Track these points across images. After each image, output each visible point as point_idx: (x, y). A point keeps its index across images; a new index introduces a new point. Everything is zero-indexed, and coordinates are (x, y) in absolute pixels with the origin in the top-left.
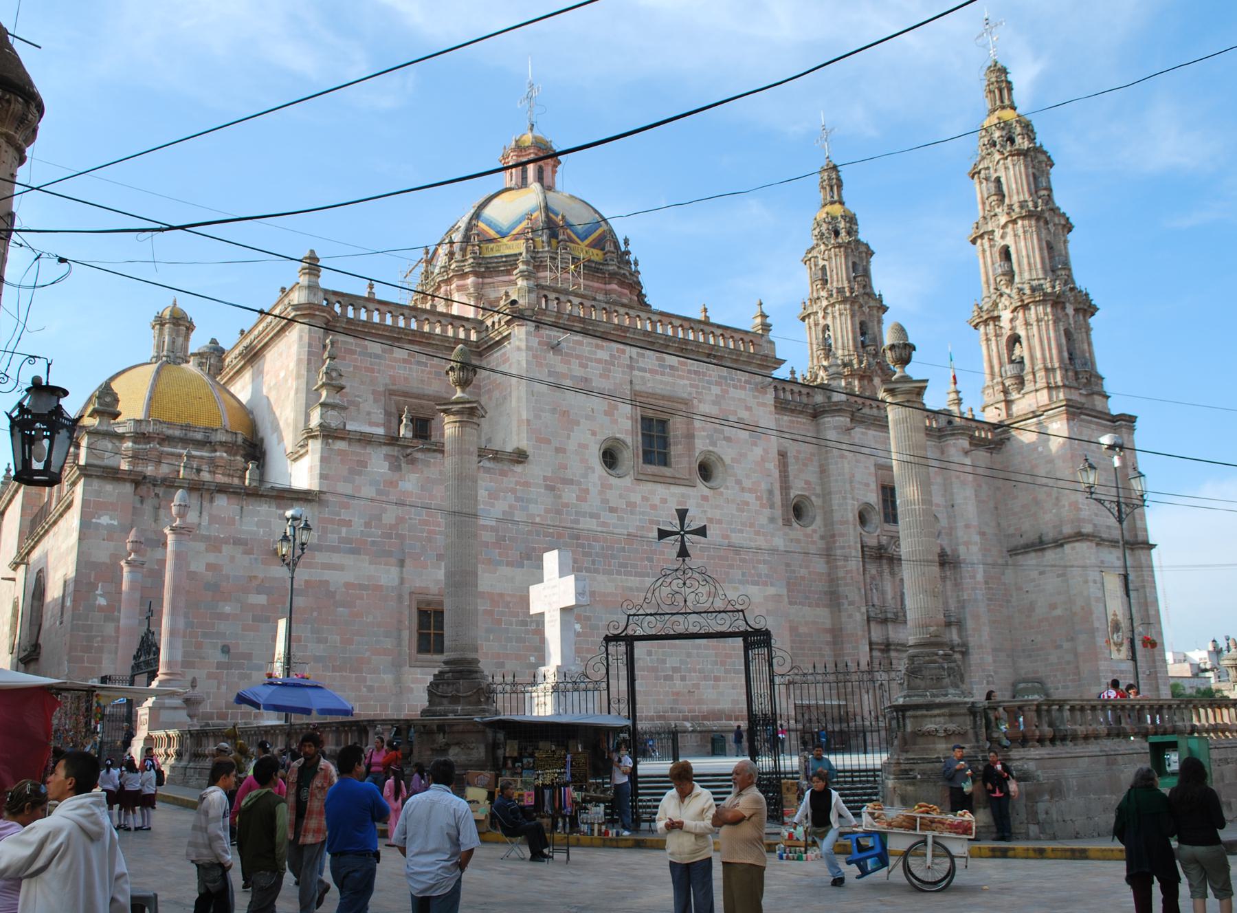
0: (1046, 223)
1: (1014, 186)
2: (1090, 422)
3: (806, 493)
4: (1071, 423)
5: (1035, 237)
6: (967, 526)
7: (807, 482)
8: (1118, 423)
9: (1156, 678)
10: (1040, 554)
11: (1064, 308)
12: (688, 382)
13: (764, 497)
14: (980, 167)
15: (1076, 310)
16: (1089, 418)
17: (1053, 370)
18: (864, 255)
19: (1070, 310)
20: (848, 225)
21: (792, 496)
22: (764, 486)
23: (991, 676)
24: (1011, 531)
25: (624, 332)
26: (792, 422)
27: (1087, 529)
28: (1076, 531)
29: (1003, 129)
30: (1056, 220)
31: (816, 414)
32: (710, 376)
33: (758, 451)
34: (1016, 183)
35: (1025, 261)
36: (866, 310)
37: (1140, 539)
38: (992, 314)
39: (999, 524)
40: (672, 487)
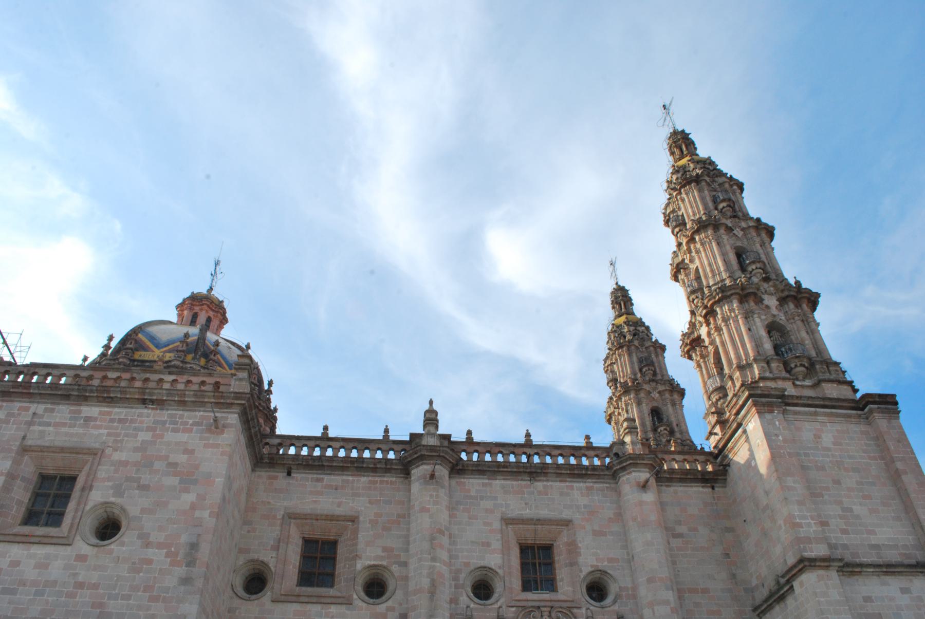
0: (729, 230)
1: (690, 210)
2: (816, 414)
3: (384, 563)
4: (768, 416)
5: (714, 244)
6: (650, 580)
7: (385, 549)
8: (866, 410)
10: (782, 605)
11: (759, 301)
12: (106, 431)
13: (182, 552)
14: (667, 213)
15: (782, 301)
17: (749, 365)
18: (652, 348)
19: (771, 301)
20: (632, 328)
21: (359, 566)
22: (184, 539)
24: (754, 582)
25: (25, 388)
26: (375, 482)
27: (819, 550)
28: (798, 557)
29: (678, 172)
30: (743, 224)
31: (404, 468)
32: (142, 422)
33: (189, 498)
34: (692, 207)
35: (708, 269)
36: (656, 395)
38: (692, 337)
39: (734, 576)
40: (35, 546)
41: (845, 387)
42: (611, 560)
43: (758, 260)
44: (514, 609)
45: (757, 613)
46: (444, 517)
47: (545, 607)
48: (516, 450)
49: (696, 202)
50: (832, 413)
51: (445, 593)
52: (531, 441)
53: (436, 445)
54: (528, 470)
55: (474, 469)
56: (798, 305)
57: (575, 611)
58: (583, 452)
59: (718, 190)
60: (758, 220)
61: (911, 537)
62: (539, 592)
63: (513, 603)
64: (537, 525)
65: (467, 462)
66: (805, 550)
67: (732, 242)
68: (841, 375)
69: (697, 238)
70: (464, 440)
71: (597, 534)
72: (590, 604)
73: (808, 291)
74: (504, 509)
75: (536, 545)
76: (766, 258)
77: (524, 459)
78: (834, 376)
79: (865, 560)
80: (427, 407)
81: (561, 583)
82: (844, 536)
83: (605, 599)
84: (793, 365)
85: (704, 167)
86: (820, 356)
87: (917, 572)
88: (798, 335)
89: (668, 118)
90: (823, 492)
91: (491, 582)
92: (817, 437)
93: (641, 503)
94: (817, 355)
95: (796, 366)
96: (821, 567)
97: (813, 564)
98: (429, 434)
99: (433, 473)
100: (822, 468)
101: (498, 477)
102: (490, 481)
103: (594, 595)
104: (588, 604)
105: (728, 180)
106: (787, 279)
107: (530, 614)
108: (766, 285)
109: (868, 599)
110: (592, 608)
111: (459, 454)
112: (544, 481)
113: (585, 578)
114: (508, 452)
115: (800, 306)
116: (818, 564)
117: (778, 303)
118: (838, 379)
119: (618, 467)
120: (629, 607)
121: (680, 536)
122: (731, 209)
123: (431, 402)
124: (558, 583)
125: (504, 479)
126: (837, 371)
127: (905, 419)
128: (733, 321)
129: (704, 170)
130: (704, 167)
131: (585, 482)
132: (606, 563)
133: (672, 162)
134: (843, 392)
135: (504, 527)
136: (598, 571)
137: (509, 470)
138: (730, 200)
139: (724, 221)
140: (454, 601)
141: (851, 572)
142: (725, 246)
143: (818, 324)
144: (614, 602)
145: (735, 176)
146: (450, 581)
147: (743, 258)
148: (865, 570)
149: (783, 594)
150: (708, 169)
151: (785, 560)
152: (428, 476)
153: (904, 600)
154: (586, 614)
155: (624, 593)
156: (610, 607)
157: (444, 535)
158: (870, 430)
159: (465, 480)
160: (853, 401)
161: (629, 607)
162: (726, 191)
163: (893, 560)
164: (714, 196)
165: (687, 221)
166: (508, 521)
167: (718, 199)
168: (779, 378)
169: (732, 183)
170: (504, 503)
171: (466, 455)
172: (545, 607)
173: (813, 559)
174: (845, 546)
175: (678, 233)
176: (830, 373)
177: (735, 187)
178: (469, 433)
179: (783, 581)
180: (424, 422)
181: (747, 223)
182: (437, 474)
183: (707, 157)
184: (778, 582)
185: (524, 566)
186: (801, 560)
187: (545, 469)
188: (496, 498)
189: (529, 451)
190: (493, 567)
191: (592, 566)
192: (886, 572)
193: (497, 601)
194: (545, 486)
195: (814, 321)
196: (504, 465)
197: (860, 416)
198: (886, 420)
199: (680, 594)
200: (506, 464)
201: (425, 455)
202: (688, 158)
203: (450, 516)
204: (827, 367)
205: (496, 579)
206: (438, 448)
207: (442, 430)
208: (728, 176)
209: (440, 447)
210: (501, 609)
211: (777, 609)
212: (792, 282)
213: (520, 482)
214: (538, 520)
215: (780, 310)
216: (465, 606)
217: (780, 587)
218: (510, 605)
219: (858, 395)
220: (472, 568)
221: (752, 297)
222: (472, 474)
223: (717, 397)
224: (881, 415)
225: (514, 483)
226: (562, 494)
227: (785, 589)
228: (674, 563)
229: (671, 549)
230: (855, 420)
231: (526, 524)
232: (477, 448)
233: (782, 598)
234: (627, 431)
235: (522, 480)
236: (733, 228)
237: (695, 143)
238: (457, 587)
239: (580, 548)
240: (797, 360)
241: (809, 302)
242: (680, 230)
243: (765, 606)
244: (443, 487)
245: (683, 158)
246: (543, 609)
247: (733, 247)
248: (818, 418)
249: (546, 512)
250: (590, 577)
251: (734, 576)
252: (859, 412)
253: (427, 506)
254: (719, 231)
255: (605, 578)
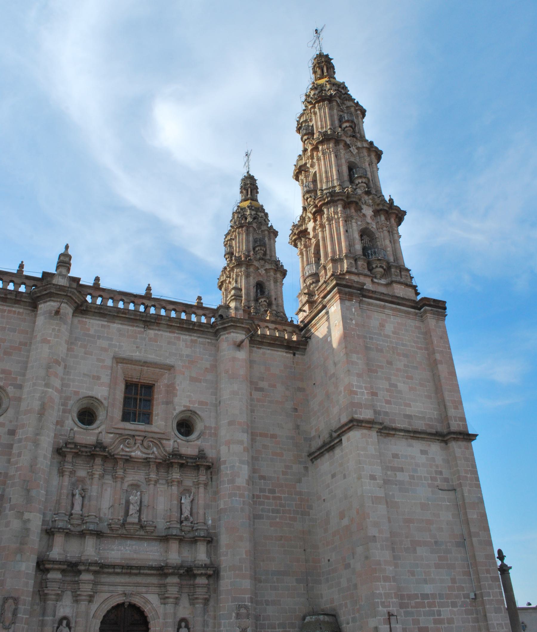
0: (347, 146)
1: (319, 123)
2: (384, 307)
4: (347, 303)
6: (230, 423)
8: (422, 310)
9: (483, 603)
11: (359, 209)
14: (301, 121)
15: (377, 213)
16: (383, 303)
17: (341, 260)
19: (368, 211)
23: (246, 607)
27: (366, 414)
28: (350, 418)
29: (316, 89)
30: (359, 144)
34: (321, 121)
35: (324, 175)
36: (262, 271)
37: (455, 426)
38: (300, 229)
41: (410, 290)
42: (201, 403)
43: (365, 176)
44: (112, 435)
45: (311, 458)
46: (62, 349)
47: (139, 436)
48: (136, 301)
49: (325, 117)
50: (396, 308)
51: (53, 415)
52: (151, 294)
53: (65, 285)
54: (144, 319)
55: (96, 311)
56: (388, 219)
57: (164, 442)
58: (193, 310)
59: (345, 111)
60: (371, 143)
61: (435, 413)
62: (136, 423)
63: (112, 430)
64: (144, 366)
65: (91, 305)
66: (356, 413)
67: (348, 157)
68: (409, 280)
69: (320, 148)
70: (92, 285)
71: (193, 380)
72: (178, 437)
73: (397, 208)
74: (117, 350)
75: (140, 384)
76: (371, 176)
77: (142, 309)
78: (404, 279)
79: (399, 425)
80: (63, 250)
81: (156, 418)
82: (387, 405)
83: (192, 434)
84: (374, 266)
85: (338, 90)
86: (396, 262)
87: (435, 439)
88: (383, 243)
89: (317, 42)
90: (378, 369)
91: (95, 410)
92: (382, 326)
93: (234, 359)
94: (394, 260)
95: (377, 267)
96: (366, 428)
97: (360, 424)
98: (60, 274)
99: (59, 310)
100: (381, 351)
101: (116, 321)
102: (109, 324)
103: (182, 430)
104: (176, 437)
105: (354, 105)
106: (383, 196)
107: (125, 441)
108: (366, 197)
109: (395, 456)
110: (179, 441)
111: (84, 296)
112: (156, 330)
113: (178, 415)
114: (128, 301)
115: (389, 219)
116: (363, 425)
117: (373, 214)
118: (406, 282)
119: (221, 327)
120: (210, 443)
121: (261, 390)
122: (352, 130)
123: (67, 247)
124: (153, 418)
125: (121, 324)
126: (406, 276)
127: (449, 321)
128: (336, 222)
129: (337, 92)
130: (338, 90)
131: (191, 336)
132: (196, 405)
133: (313, 80)
134: (408, 293)
135: (115, 365)
136: (189, 410)
137: (127, 316)
138: (352, 122)
139: (344, 138)
140: (60, 423)
141: (387, 434)
142: (341, 159)
143: (400, 237)
144: (198, 438)
145: (361, 103)
146: (59, 405)
147: (353, 172)
148: (398, 433)
149: (333, 445)
150: (341, 92)
151: (340, 419)
152: (54, 312)
153: (422, 459)
154: (174, 445)
155: (207, 432)
156: (194, 441)
157: (60, 366)
158: (422, 326)
159: (87, 320)
160: (414, 301)
161: (210, 443)
162: (351, 114)
163: (420, 428)
164: (341, 116)
165: (315, 131)
166: (119, 360)
167: (343, 119)
168: (362, 274)
169: (357, 108)
170: (118, 344)
171: (91, 298)
172: (139, 436)
173: (361, 420)
174: (386, 413)
175: (306, 140)
176: (401, 277)
177: (359, 112)
178: (97, 279)
179: (335, 435)
180: (58, 263)
181: (362, 144)
182: (61, 311)
183: (342, 82)
184: (331, 436)
185: (127, 400)
186: (352, 421)
187: (158, 320)
188: (111, 339)
189: (147, 302)
190: (99, 398)
191: (185, 406)
192: (413, 437)
193: (98, 427)
194: (155, 334)
195: (398, 233)
196: (123, 312)
197: (416, 314)
198: (435, 320)
199: (253, 436)
200: (126, 311)
201: (53, 293)
202: (326, 79)
203: (68, 350)
204: (400, 271)
205: (100, 409)
206: (67, 289)
207: (73, 273)
208: (356, 101)
209: (69, 288)
210: (101, 434)
211: (327, 456)
212: (387, 199)
213: (135, 328)
214: (145, 362)
215: (373, 220)
216: (69, 429)
217: (332, 439)
218: (109, 431)
219: (419, 298)
220: (81, 396)
221: (354, 205)
222: (93, 316)
223: (311, 281)
224: (432, 315)
225: (130, 328)
226: (169, 343)
227: (336, 441)
228: (252, 411)
229: (252, 400)
230: (413, 317)
231: (134, 365)
232: (101, 293)
233: (332, 448)
234: (233, 297)
235: (137, 326)
236: (350, 146)
237: (335, 68)
238: (64, 411)
239: (177, 390)
240: (378, 262)
241: (396, 218)
242: (308, 138)
243: (318, 453)
244: (65, 324)
245: (323, 78)
246: (137, 438)
247: (347, 161)
248: (386, 310)
249: (153, 356)
250: (182, 416)
251: (298, 427)
252: (417, 311)
253: (48, 339)
254: (339, 146)
255: (194, 417)
